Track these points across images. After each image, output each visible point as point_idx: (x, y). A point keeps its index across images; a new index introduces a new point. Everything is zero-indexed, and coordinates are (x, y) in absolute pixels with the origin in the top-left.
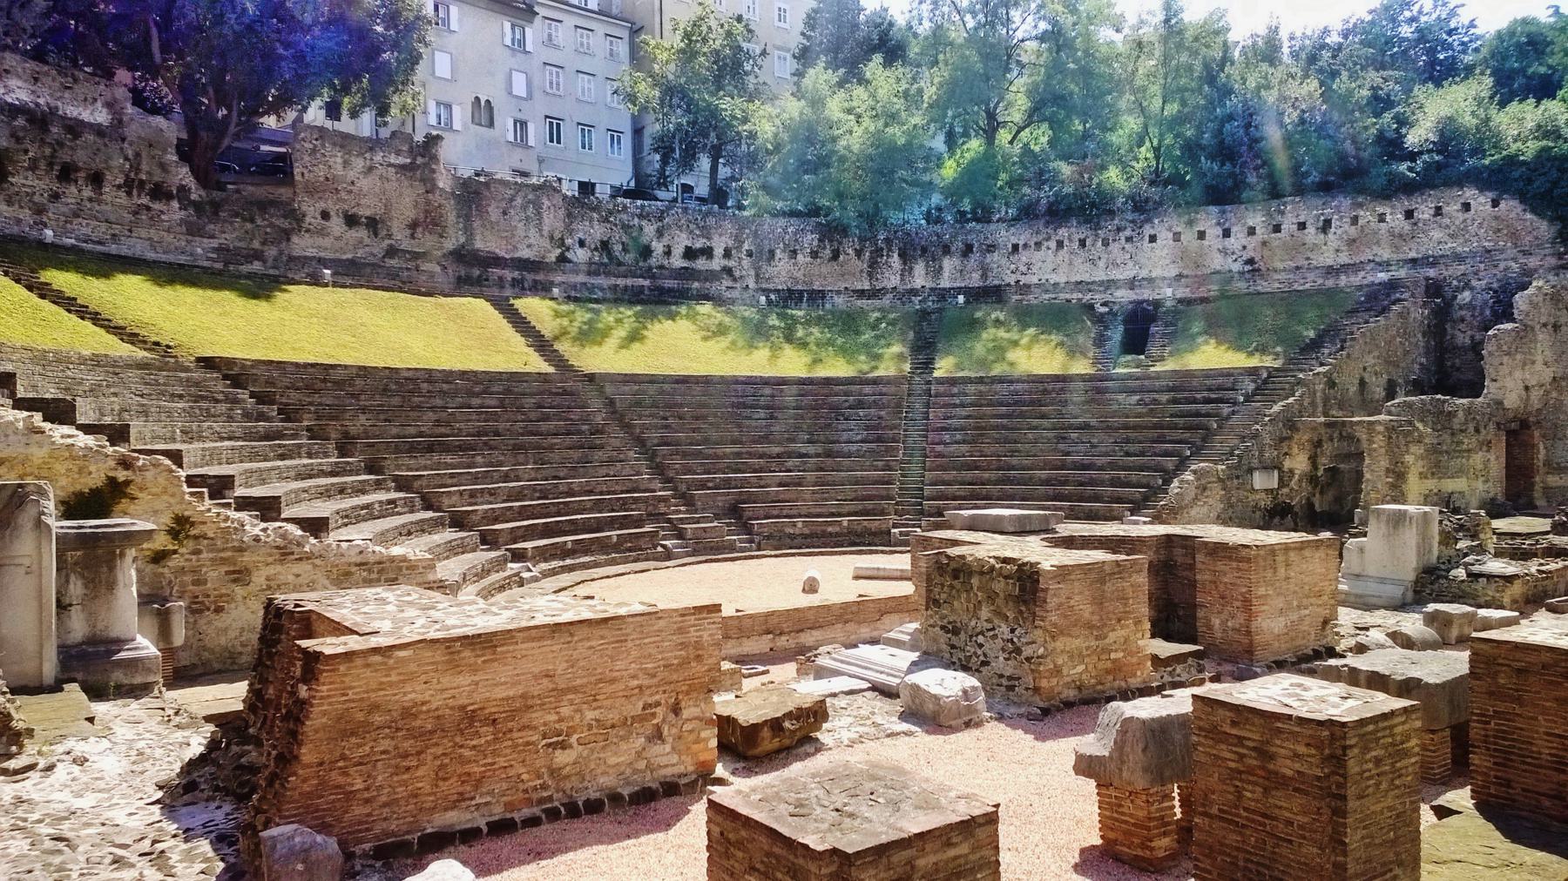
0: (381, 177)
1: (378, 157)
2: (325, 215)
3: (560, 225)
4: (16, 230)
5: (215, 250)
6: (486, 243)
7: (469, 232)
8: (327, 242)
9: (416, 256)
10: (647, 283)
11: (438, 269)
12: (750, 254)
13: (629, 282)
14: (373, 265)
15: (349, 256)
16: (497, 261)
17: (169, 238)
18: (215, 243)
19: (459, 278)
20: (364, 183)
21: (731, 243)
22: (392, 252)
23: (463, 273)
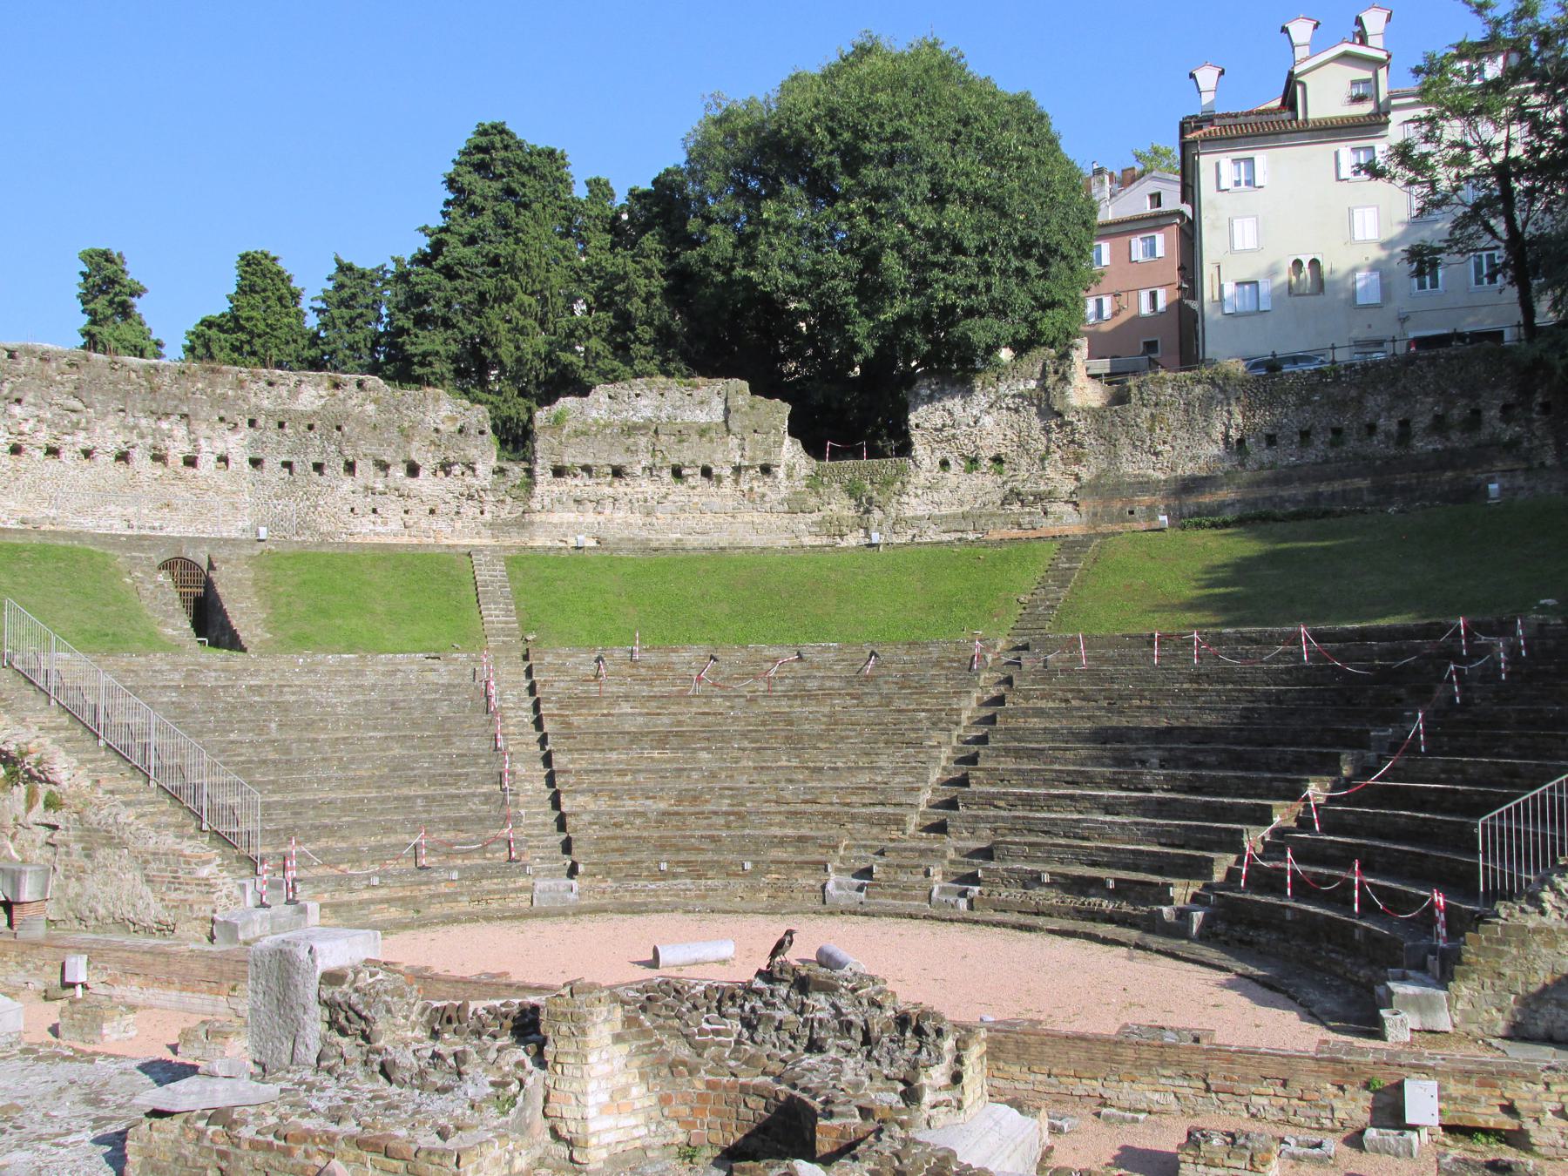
0: (1009, 409)
1: (1003, 388)
2: (944, 464)
3: (1239, 419)
4: (626, 534)
5: (819, 524)
6: (1134, 465)
7: (1113, 457)
8: (943, 495)
9: (1039, 497)
10: (1363, 483)
11: (1070, 507)
12: (1546, 408)
13: (1337, 486)
14: (992, 515)
15: (967, 508)
16: (1144, 486)
17: (773, 518)
18: (816, 517)
19: (1095, 514)
20: (987, 421)
21: (1511, 397)
22: (1015, 495)
23: (1100, 509)
